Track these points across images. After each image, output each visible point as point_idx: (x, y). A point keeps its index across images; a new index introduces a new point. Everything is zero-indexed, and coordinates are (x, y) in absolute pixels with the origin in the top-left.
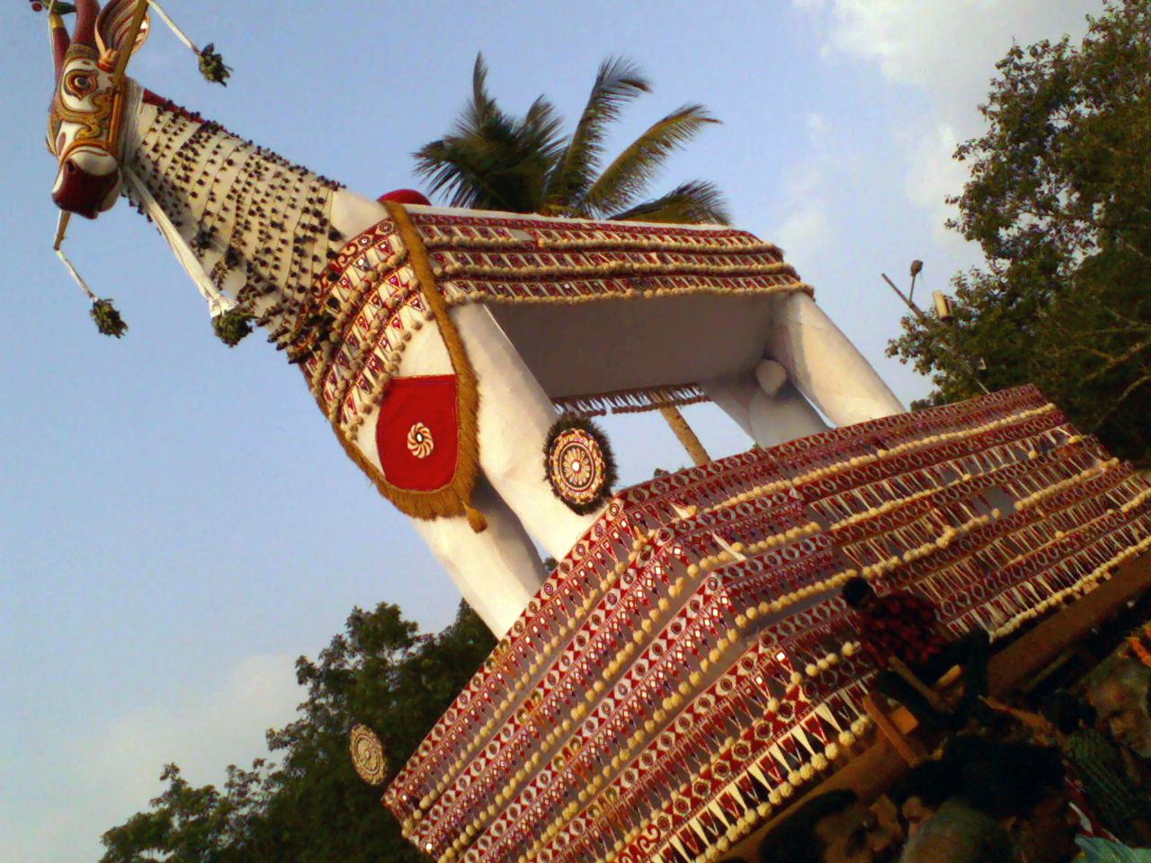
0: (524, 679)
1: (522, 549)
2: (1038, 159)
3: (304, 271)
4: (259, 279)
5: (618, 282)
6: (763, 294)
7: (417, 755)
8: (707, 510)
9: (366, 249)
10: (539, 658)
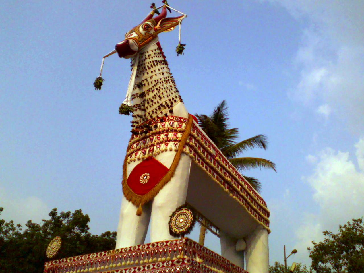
0: (114, 265)
1: (144, 230)
2: (344, 252)
3: (156, 113)
4: (144, 105)
5: (226, 185)
6: (257, 222)
7: (67, 259)
8: (204, 265)
9: (175, 121)
10: (123, 263)
